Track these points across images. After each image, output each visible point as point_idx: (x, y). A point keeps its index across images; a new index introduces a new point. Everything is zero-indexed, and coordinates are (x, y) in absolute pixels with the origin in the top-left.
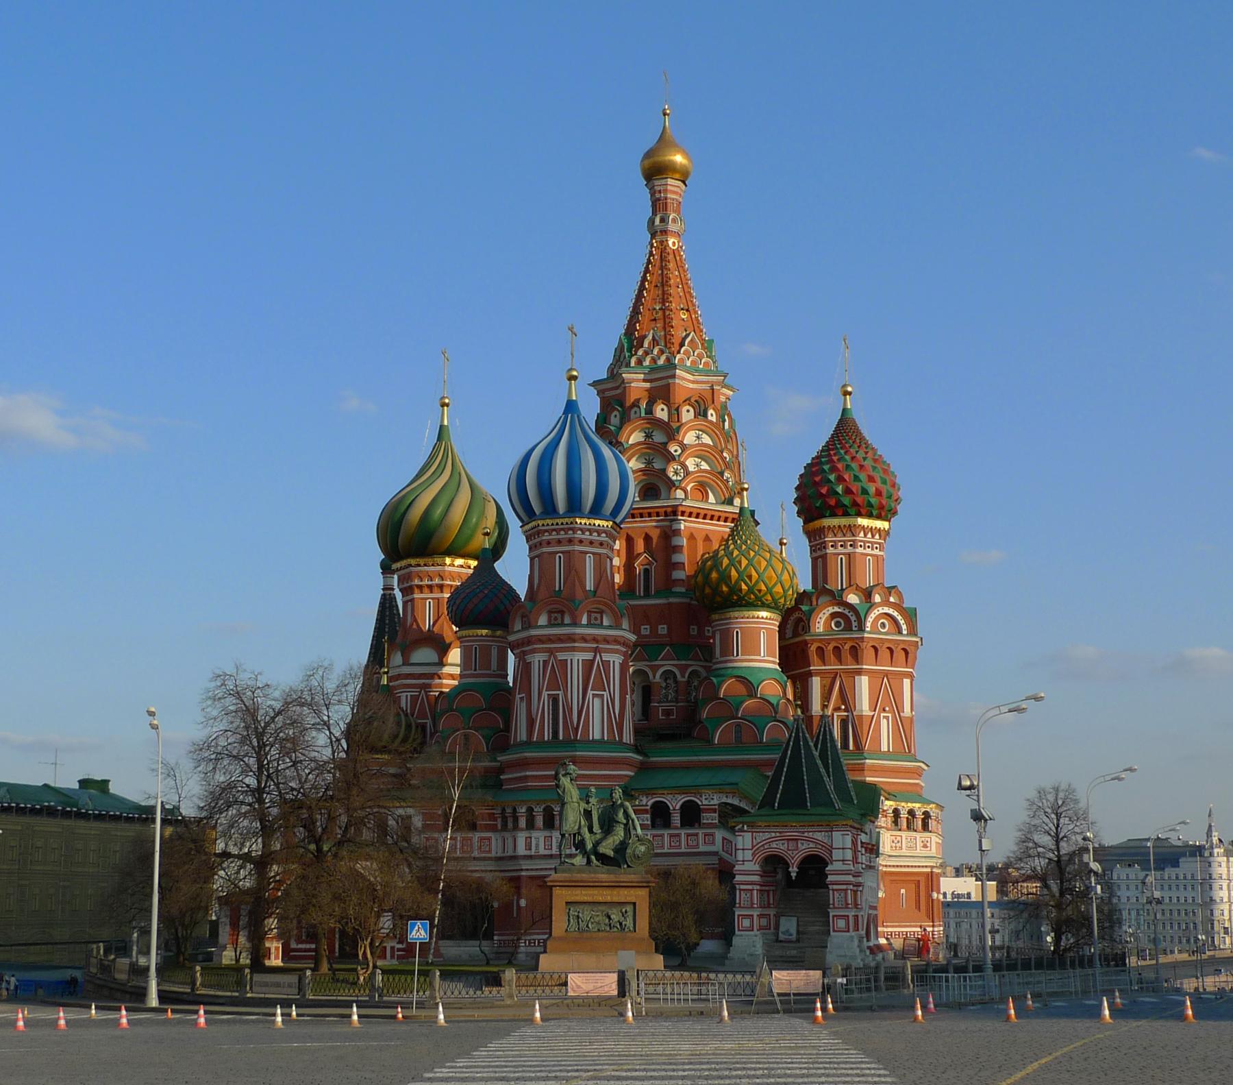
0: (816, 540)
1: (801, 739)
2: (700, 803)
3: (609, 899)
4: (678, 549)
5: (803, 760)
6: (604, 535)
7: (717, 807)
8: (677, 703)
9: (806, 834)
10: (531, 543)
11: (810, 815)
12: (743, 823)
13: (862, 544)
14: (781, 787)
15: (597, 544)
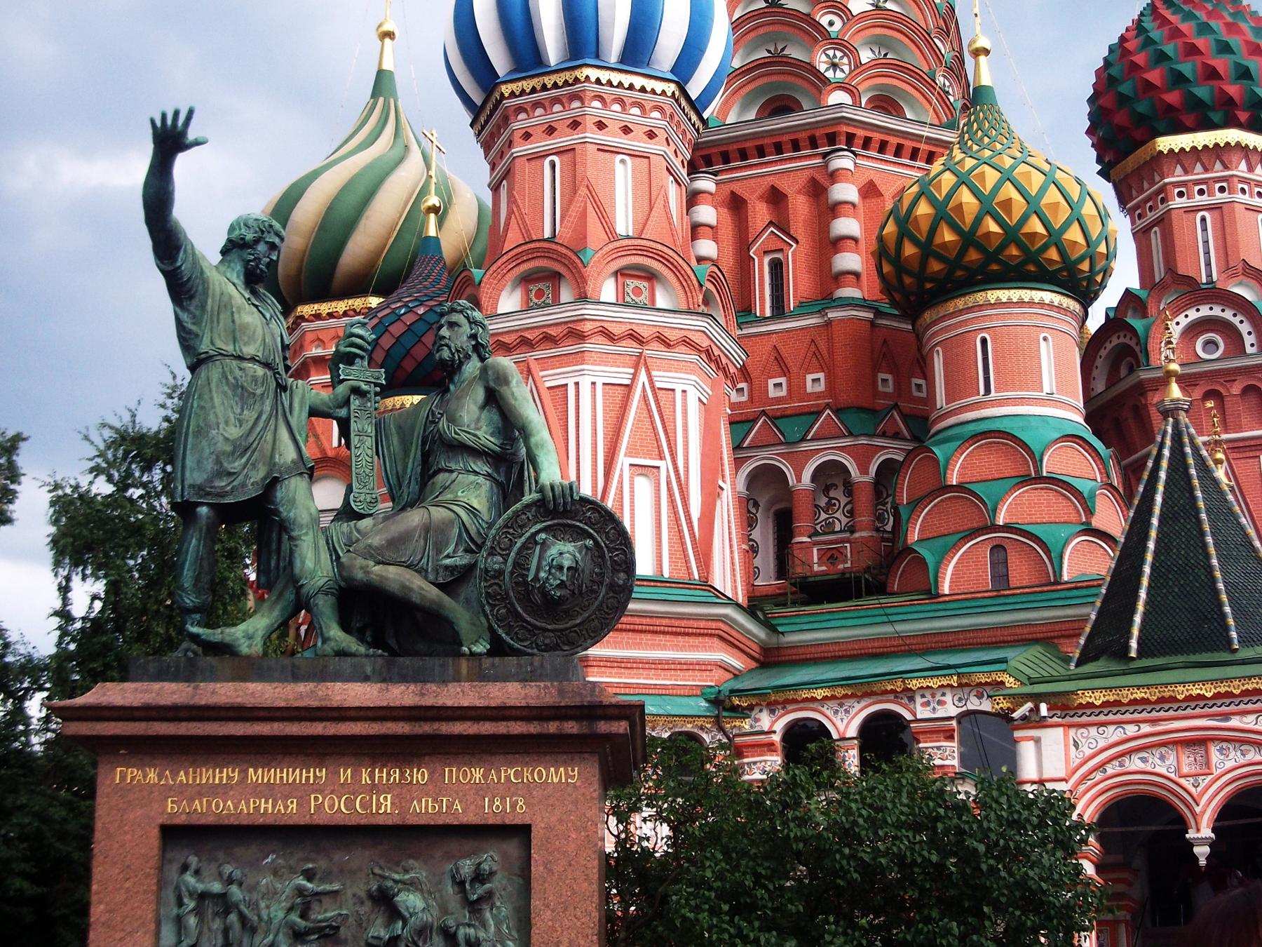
0: (1142, 191)
1: (1191, 461)
2: (908, 716)
3: (385, 807)
4: (835, 210)
5: (1204, 516)
6: (656, 114)
7: (954, 723)
8: (852, 530)
9: (1235, 722)
10: (492, 153)
11: (1244, 662)
12: (1037, 698)
13: (1246, 187)
14: (1143, 594)
15: (639, 132)
